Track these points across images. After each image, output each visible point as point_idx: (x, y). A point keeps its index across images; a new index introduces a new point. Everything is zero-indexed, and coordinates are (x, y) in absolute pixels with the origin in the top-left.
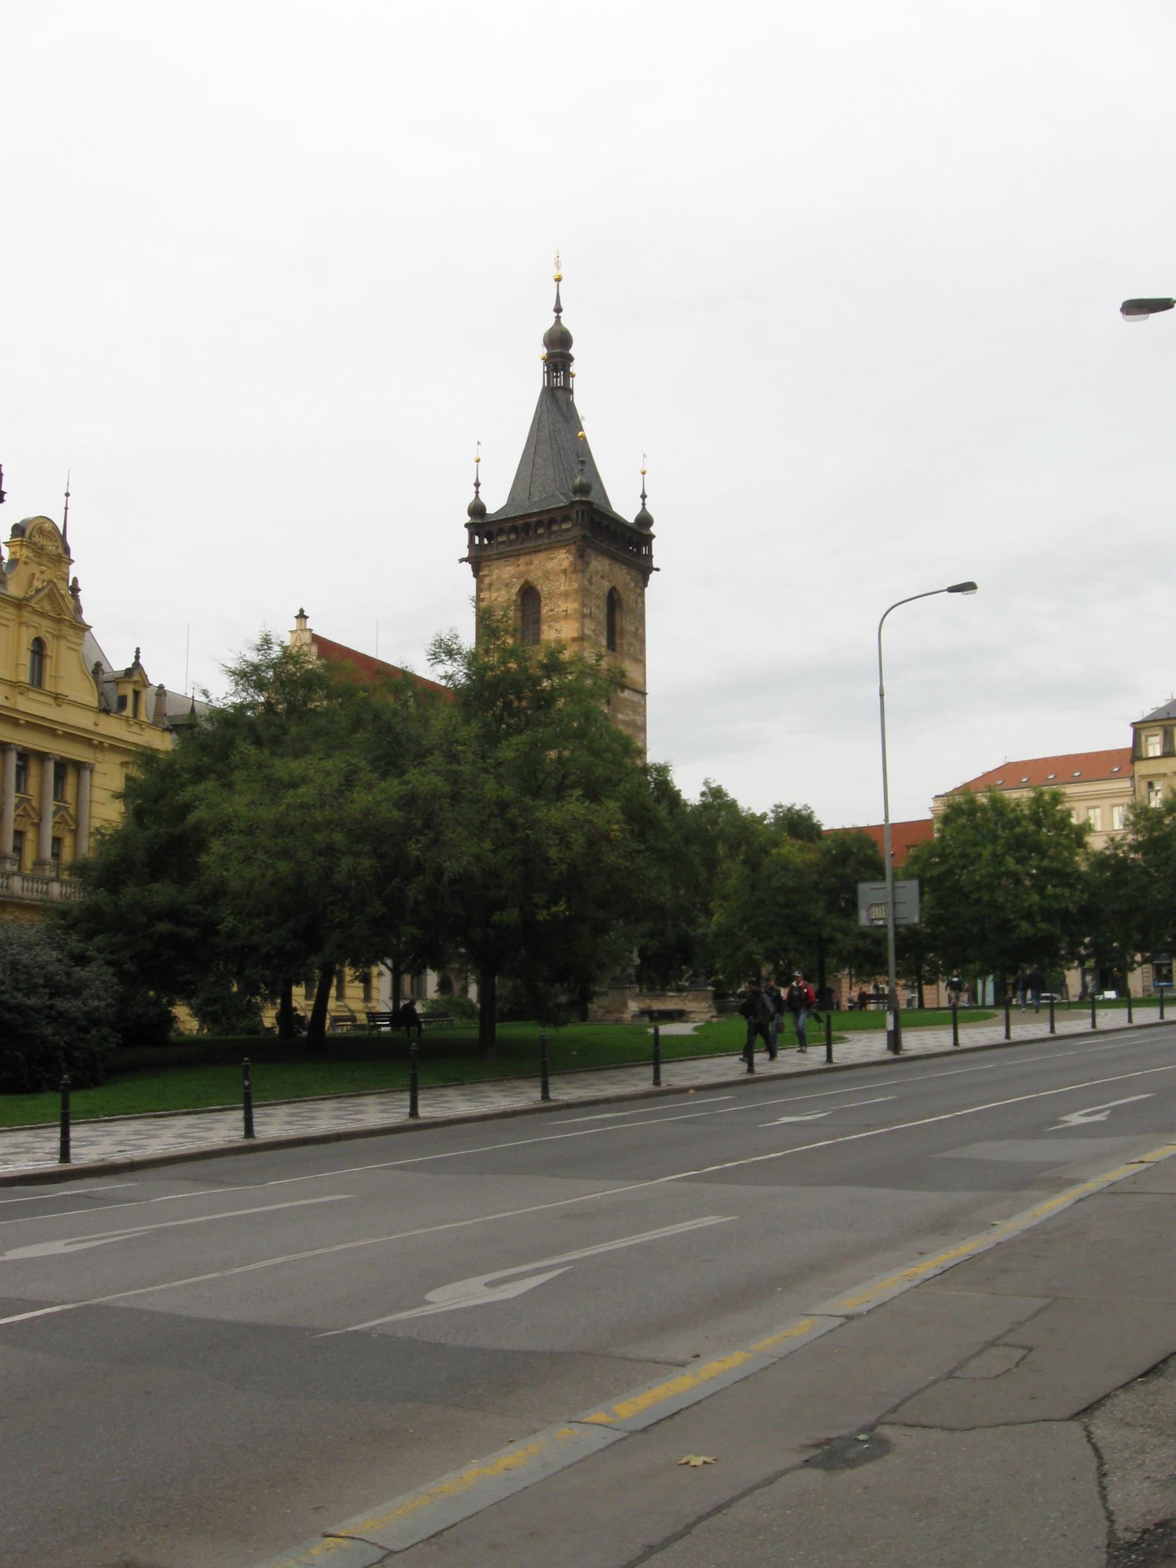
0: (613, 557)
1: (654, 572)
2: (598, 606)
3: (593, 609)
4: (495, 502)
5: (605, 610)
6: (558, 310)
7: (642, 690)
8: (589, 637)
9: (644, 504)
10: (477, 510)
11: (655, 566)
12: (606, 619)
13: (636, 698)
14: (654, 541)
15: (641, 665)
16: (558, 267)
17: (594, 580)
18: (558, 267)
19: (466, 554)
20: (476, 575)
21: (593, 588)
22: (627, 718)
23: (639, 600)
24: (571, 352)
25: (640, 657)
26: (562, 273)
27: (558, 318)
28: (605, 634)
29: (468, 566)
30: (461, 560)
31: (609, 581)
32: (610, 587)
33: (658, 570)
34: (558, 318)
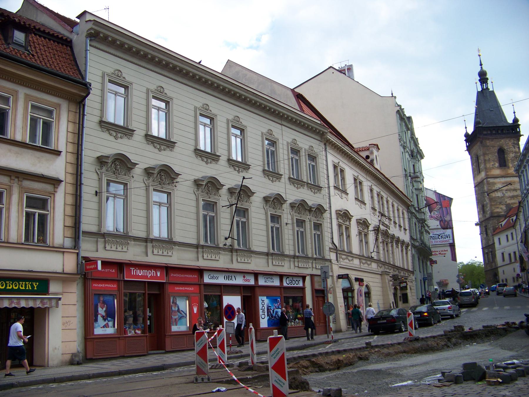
1: (522, 136)
4: (470, 130)
6: (481, 65)
9: (515, 115)
10: (466, 135)
11: (521, 134)
14: (520, 126)
16: (479, 52)
18: (479, 52)
19: (466, 149)
20: (469, 155)
24: (487, 77)
26: (480, 54)
27: (481, 67)
29: (467, 152)
33: (523, 135)
34: (481, 67)
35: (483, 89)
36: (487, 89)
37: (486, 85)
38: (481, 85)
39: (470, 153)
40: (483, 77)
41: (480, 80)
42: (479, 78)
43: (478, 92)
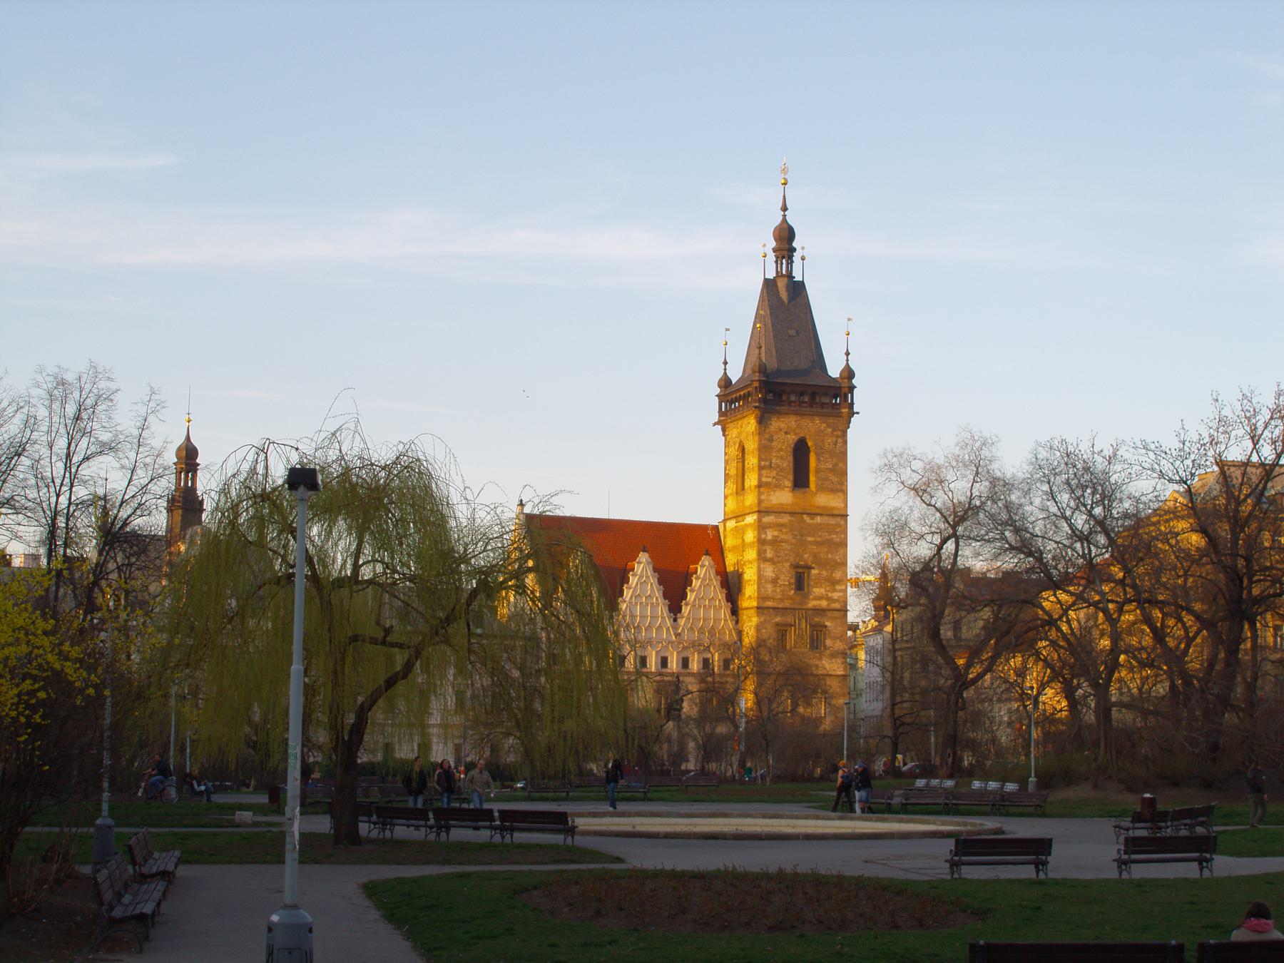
0: (802, 415)
2: (781, 458)
3: (774, 461)
5: (791, 458)
6: (785, 209)
7: (843, 513)
8: (767, 484)
9: (847, 360)
10: (725, 383)
12: (791, 465)
13: (832, 521)
15: (841, 494)
17: (775, 437)
19: (716, 418)
20: (724, 435)
21: (773, 444)
22: (819, 539)
23: (840, 440)
25: (838, 487)
28: (791, 477)
30: (715, 424)
31: (796, 434)
32: (796, 439)
33: (858, 413)
35: (779, 274)
36: (790, 276)
37: (788, 264)
38: (776, 262)
39: (724, 430)
40: (785, 239)
41: (775, 250)
42: (774, 244)
43: (766, 281)
